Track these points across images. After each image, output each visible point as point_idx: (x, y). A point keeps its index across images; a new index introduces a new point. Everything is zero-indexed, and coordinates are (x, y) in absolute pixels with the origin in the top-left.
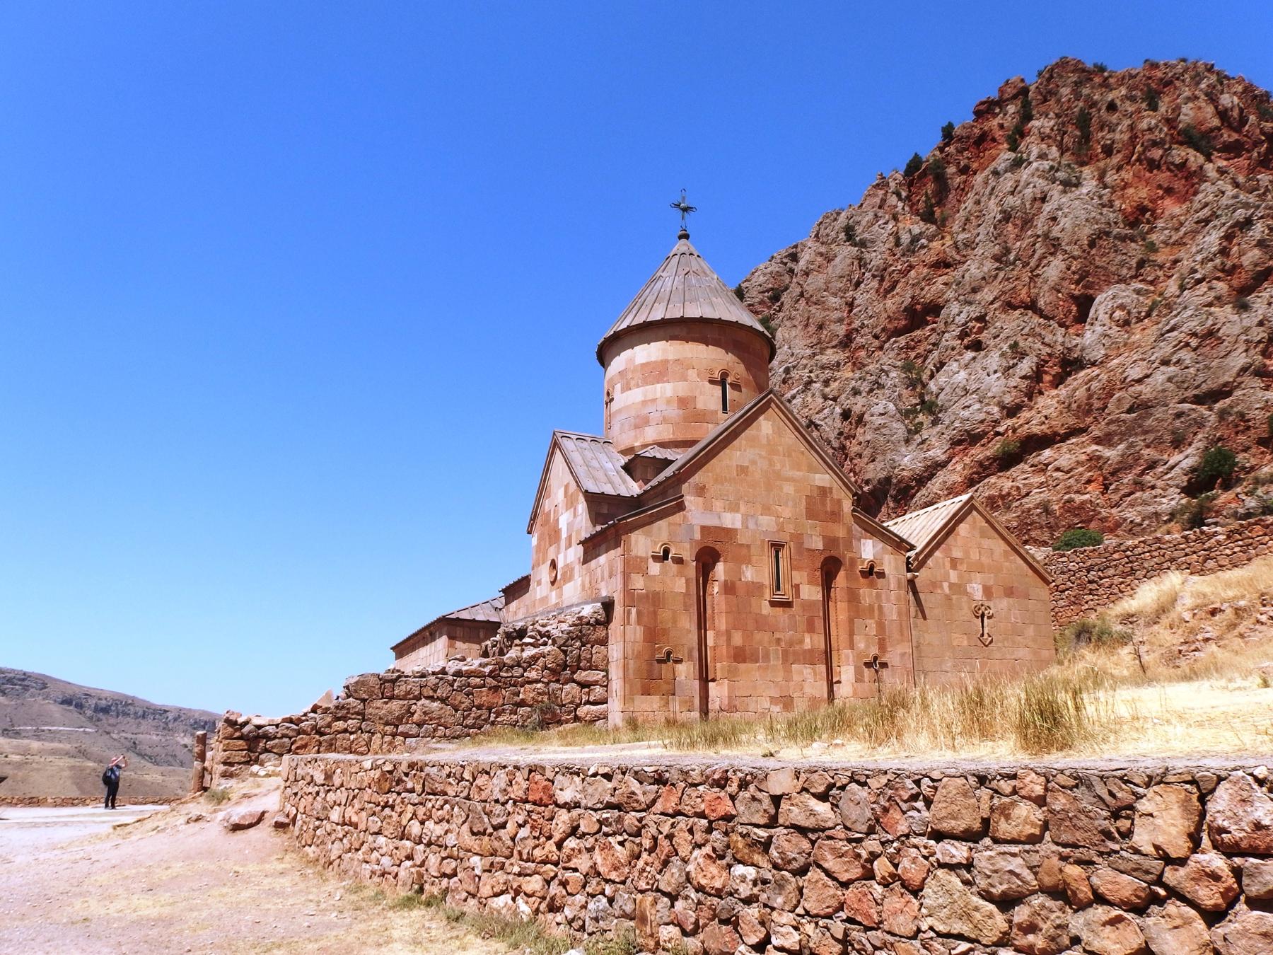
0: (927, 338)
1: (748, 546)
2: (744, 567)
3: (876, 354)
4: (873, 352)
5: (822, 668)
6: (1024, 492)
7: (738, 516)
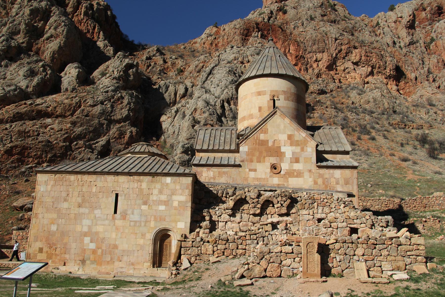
6: (36, 133)
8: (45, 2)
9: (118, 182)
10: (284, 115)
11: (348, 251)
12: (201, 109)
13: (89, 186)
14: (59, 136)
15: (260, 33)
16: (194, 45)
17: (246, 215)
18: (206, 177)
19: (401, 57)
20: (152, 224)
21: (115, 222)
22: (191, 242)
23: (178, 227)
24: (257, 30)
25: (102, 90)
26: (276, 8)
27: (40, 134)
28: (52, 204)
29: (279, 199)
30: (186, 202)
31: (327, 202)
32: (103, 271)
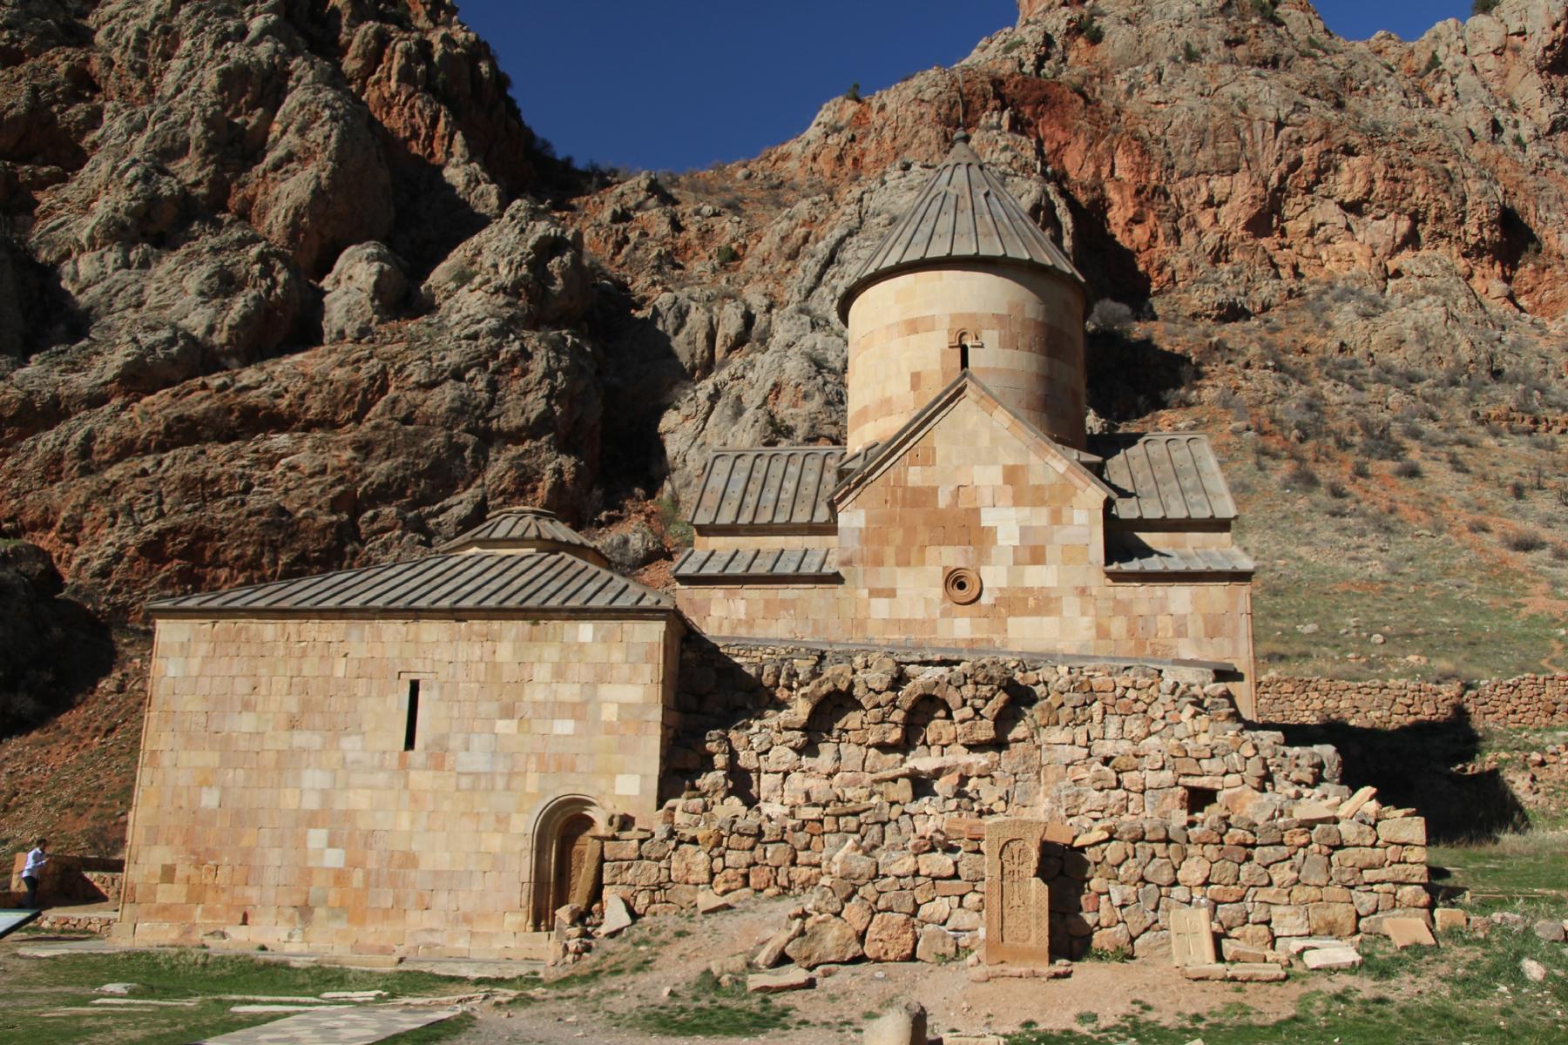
6: (240, 485)
8: (269, 45)
9: (417, 641)
10: (991, 399)
11: (1150, 868)
12: (797, 385)
13: (322, 657)
14: (316, 490)
15: (1006, 114)
16: (779, 164)
17: (853, 748)
18: (721, 619)
19: (1521, 176)
20: (532, 782)
21: (407, 775)
22: (635, 843)
23: (618, 791)
24: (998, 103)
25: (456, 332)
26: (1063, 26)
27: (252, 486)
28: (203, 719)
29: (968, 691)
30: (646, 705)
31: (1136, 700)
32: (370, 940)
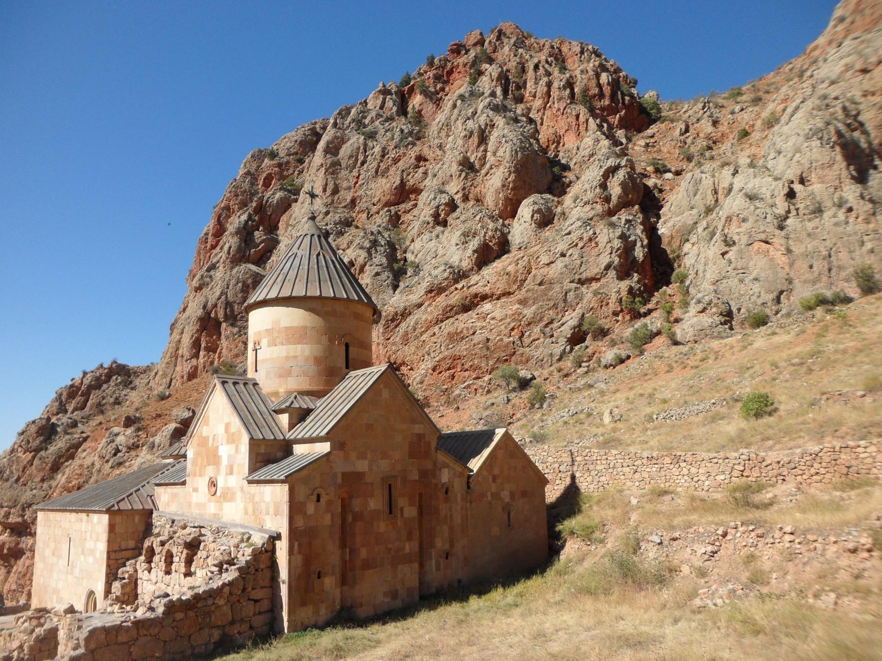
0: (409, 211)
1: (372, 484)
2: (369, 499)
3: (374, 217)
4: (372, 215)
5: (416, 565)
6: (471, 332)
7: (367, 462)
14: (503, 327)
16: (811, 55)
